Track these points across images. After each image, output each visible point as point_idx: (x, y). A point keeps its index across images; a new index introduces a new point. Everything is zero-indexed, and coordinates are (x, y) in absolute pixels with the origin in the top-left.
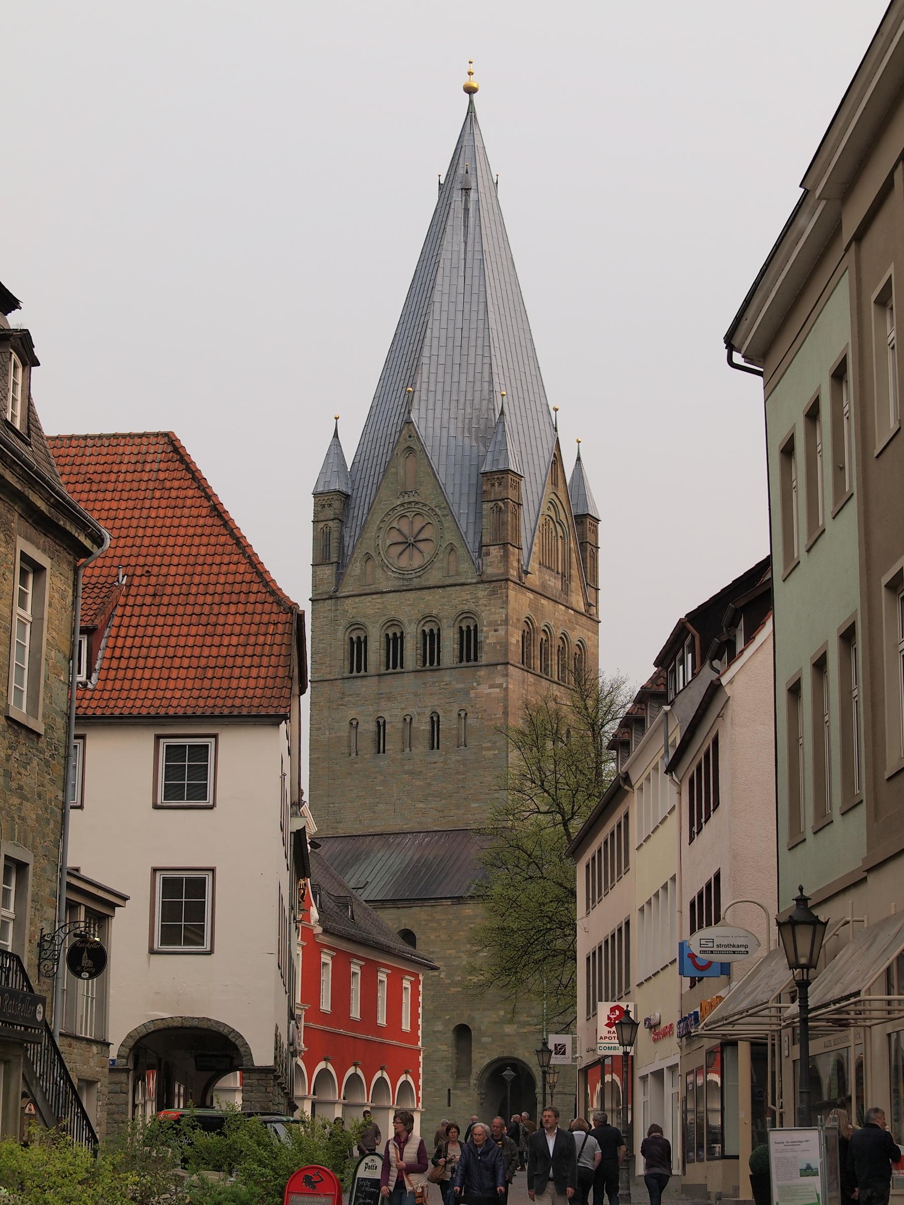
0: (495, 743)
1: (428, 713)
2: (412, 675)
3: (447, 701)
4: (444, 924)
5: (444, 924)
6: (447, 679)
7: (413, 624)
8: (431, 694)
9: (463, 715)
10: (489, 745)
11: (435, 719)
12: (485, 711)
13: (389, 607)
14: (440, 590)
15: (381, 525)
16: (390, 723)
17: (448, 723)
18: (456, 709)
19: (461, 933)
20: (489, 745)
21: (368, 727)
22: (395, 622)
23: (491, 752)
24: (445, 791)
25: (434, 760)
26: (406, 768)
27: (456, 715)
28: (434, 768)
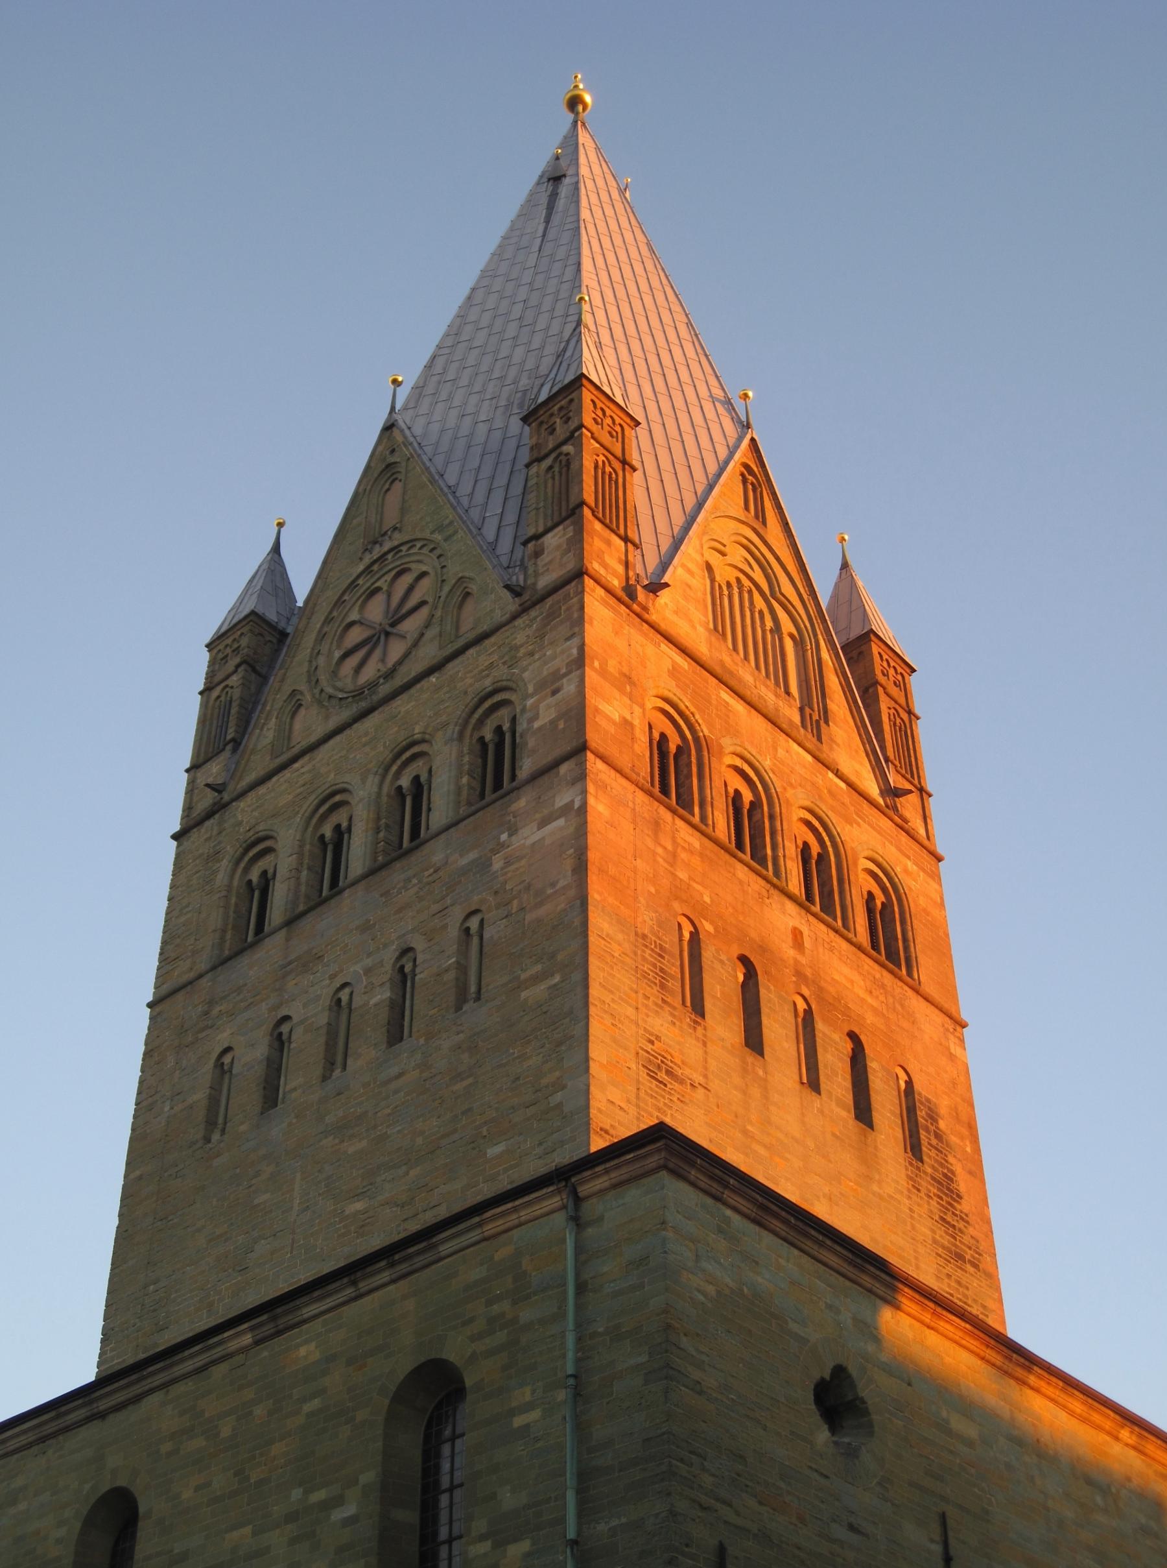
0: (553, 956)
1: (389, 956)
2: (361, 887)
3: (435, 908)
4: (226, 1431)
5: (226, 1431)
6: (438, 858)
7: (371, 777)
8: (400, 910)
9: (474, 923)
10: (539, 967)
11: (407, 969)
12: (528, 888)
13: (323, 770)
14: (433, 679)
15: (326, 629)
16: (301, 1022)
17: (435, 963)
18: (458, 913)
19: (277, 1449)
20: (539, 967)
21: (252, 1055)
22: (337, 798)
23: (543, 986)
24: (419, 1141)
25: (394, 1071)
26: (329, 1119)
27: (454, 932)
28: (396, 1092)
